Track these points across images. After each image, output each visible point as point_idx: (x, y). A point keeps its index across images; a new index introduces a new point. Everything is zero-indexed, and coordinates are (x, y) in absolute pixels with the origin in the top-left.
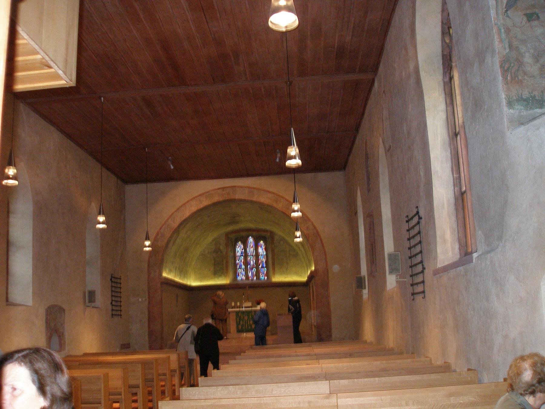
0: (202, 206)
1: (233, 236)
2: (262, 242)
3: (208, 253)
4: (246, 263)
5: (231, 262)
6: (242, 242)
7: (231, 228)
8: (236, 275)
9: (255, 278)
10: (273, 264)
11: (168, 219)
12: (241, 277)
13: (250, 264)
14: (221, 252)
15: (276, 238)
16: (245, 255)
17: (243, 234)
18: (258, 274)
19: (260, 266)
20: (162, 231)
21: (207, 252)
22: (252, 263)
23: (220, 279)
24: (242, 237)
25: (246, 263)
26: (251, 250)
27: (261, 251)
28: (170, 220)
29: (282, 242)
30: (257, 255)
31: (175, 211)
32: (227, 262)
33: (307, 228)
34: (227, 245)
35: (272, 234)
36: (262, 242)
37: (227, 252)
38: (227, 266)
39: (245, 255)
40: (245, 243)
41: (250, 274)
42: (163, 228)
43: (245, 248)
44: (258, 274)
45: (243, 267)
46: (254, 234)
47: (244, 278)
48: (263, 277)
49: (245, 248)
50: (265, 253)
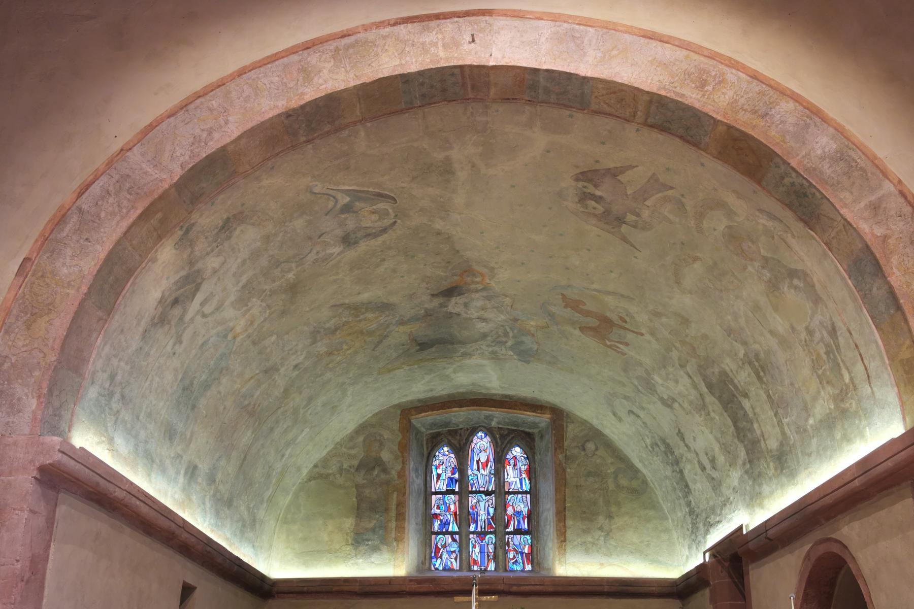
0: (311, 93)
1: (424, 421)
2: (517, 451)
3: (341, 470)
4: (465, 516)
5: (413, 506)
6: (450, 445)
7: (420, 385)
8: (429, 552)
9: (492, 567)
10: (561, 515)
11: (124, 150)
12: (447, 561)
13: (476, 521)
14: (385, 470)
15: (571, 431)
16: (462, 487)
17: (459, 416)
18: (500, 553)
19: (511, 529)
20: (85, 202)
21: (333, 468)
22: (483, 516)
23: (375, 558)
24: (453, 433)
25: (465, 516)
26: (480, 477)
27: (514, 477)
28: (135, 156)
29: (590, 446)
30: (501, 492)
31: (172, 114)
32: (401, 505)
33: (875, 208)
34: (403, 448)
35: (558, 415)
36: (517, 451)
37: (403, 469)
38: (401, 516)
39: (462, 487)
40: (461, 451)
41: (476, 554)
42: (96, 189)
43: (462, 467)
44: (500, 553)
45: (453, 527)
46: (498, 416)
47: (456, 565)
48: (519, 566)
49: (462, 467)
50: (526, 487)
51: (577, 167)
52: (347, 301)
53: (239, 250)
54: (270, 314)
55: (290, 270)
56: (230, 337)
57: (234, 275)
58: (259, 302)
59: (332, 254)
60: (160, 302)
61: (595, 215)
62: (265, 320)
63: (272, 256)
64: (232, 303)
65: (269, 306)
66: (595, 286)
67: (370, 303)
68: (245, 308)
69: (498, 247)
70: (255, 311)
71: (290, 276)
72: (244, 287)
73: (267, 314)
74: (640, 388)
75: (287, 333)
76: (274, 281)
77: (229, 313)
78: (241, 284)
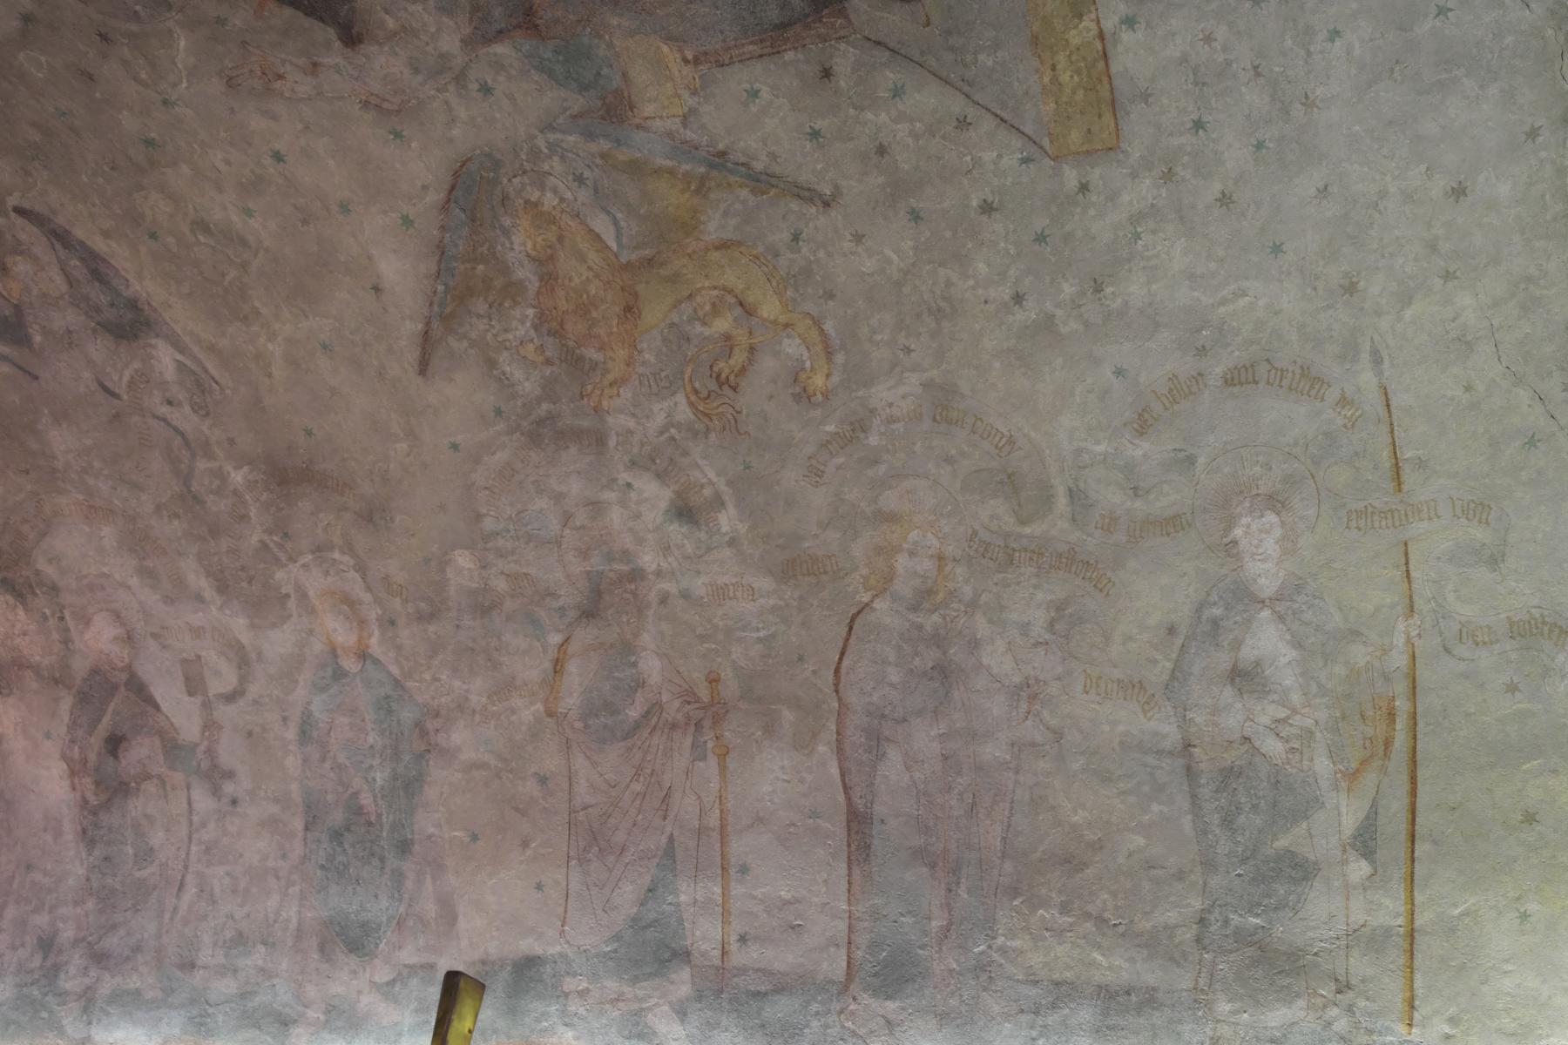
53: (103, 575)
54: (349, 548)
56: (350, 664)
57: (168, 600)
58: (294, 568)
60: (73, 773)
64: (252, 626)
67: (441, 250)
68: (292, 604)
70: (315, 582)
72: (222, 588)
73: (347, 559)
75: (479, 517)
77: (279, 642)
78: (209, 592)
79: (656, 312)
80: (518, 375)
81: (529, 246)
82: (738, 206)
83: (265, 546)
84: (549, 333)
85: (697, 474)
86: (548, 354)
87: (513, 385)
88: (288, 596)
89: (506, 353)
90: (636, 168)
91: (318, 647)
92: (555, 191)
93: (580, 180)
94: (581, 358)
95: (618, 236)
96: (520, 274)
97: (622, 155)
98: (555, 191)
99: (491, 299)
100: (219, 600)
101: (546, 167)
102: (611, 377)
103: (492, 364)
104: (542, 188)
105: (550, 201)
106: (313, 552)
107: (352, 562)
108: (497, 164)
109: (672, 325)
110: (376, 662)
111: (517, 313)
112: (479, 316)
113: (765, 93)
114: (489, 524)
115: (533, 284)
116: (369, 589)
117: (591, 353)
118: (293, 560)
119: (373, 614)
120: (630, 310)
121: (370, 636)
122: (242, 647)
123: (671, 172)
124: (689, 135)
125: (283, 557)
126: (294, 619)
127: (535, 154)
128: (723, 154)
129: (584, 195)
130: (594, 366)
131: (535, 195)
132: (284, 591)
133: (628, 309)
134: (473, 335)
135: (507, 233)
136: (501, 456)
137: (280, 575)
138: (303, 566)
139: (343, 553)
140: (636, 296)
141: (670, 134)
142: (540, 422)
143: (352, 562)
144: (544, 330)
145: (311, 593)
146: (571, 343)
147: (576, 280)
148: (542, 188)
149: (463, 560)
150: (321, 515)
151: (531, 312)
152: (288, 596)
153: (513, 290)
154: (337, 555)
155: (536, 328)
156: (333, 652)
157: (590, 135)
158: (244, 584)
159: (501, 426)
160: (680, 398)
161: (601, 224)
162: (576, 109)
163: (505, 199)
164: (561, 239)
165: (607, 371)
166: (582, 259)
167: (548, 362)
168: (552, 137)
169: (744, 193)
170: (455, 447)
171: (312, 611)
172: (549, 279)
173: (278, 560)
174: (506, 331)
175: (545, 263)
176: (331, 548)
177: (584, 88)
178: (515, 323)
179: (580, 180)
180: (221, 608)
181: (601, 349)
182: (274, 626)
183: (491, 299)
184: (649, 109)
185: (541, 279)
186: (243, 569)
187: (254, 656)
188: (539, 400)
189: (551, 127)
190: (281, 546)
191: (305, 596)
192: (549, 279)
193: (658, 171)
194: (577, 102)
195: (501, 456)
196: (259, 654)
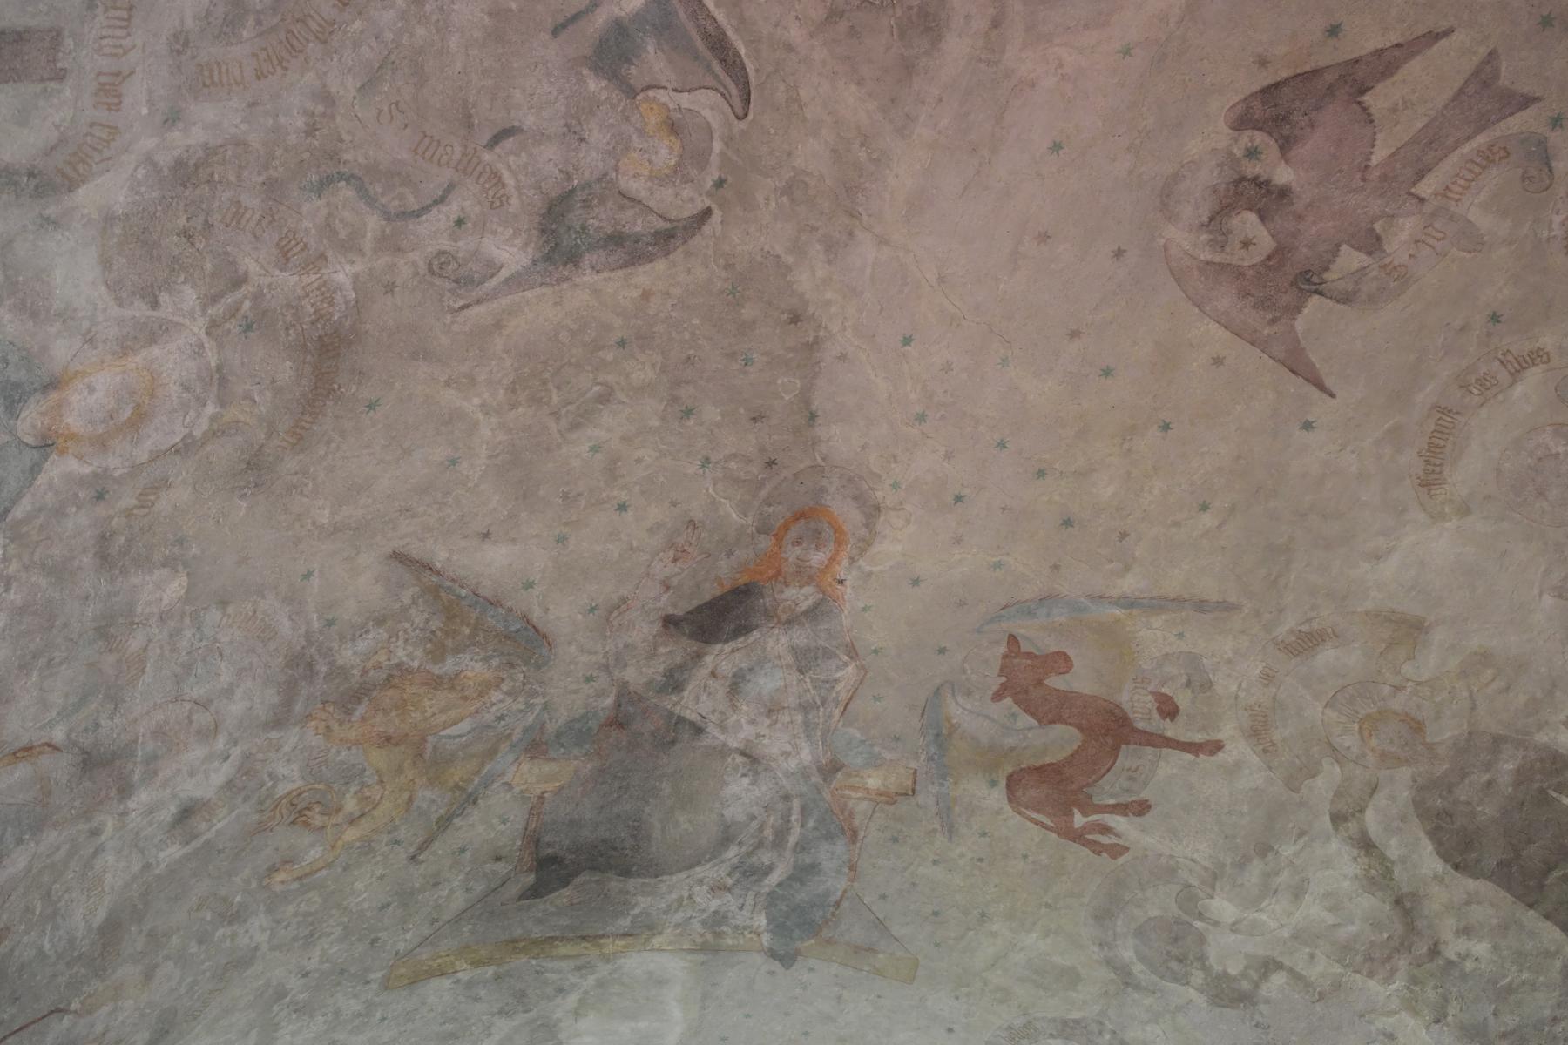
51: (1263, 63)
52: (440, 556)
54: (217, 432)
55: (350, 246)
58: (198, 327)
59: (493, 268)
61: (1238, 273)
62: (185, 448)
63: (328, 99)
64: (109, 219)
65: (220, 379)
66: (1129, 584)
68: (140, 310)
69: (921, 418)
70: (173, 361)
71: (343, 274)
72: (186, 174)
73: (204, 424)
74: (1138, 968)
75: (223, 604)
76: (284, 257)
79: (378, 758)
80: (362, 645)
81: (469, 674)
82: (434, 808)
83: (238, 282)
84: (391, 676)
85: (225, 811)
86: (372, 673)
87: (353, 640)
88: (155, 305)
89: (386, 636)
90: (492, 753)
91: (62, 350)
92: (501, 701)
93: (501, 718)
94: (359, 701)
95: (449, 737)
96: (450, 661)
97: (504, 747)
98: (501, 701)
99: (439, 633)
100: (164, 159)
101: (521, 699)
102: (335, 726)
103: (380, 622)
104: (508, 693)
105: (496, 696)
106: (219, 369)
107: (197, 433)
108: (538, 667)
109: (364, 770)
110: (35, 470)
111: (419, 653)
112: (427, 621)
113: (502, 827)
114: (214, 615)
115: (437, 670)
116: (155, 457)
117: (361, 710)
118: (213, 326)
119: (115, 462)
120: (388, 740)
121: (79, 457)
122: (72, 186)
123: (478, 772)
124: (496, 785)
125: (216, 310)
126: (115, 311)
127: (533, 694)
128: (475, 802)
129: (488, 717)
130: (349, 712)
131: (504, 687)
132: (164, 297)
133: (388, 739)
134: (413, 611)
135: (486, 659)
136: (286, 626)
137: (190, 296)
138: (202, 346)
139: (213, 419)
140: (397, 744)
141: (503, 774)
142: (310, 665)
143: (197, 433)
144: (395, 672)
145: (156, 351)
146: (374, 694)
147: (427, 703)
148: (508, 693)
149: (175, 588)
150: (268, 394)
151: (416, 664)
152: (155, 305)
153: (438, 654)
154: (211, 409)
155: (399, 666)
156: (53, 384)
157: (526, 731)
158: (182, 221)
159: (316, 625)
160: (299, 783)
161: (464, 726)
162: (548, 726)
163: (512, 666)
164: (465, 698)
165: (341, 723)
166: (442, 711)
167: (365, 672)
168: (538, 708)
169: (442, 812)
170: (308, 575)
171: (124, 349)
172: (437, 683)
173: (215, 299)
174: (406, 640)
175: (452, 682)
176: (222, 403)
177: (558, 735)
178: (410, 649)
179: (501, 718)
180: (149, 160)
181: (363, 719)
182: (106, 263)
183: (439, 633)
184: (525, 767)
185: (439, 677)
186: (208, 226)
187: (52, 211)
188: (332, 663)
189: (546, 707)
190: (234, 311)
191: (152, 340)
192: (437, 683)
193: (483, 765)
194: (551, 728)
195: (286, 626)
196: (55, 223)
